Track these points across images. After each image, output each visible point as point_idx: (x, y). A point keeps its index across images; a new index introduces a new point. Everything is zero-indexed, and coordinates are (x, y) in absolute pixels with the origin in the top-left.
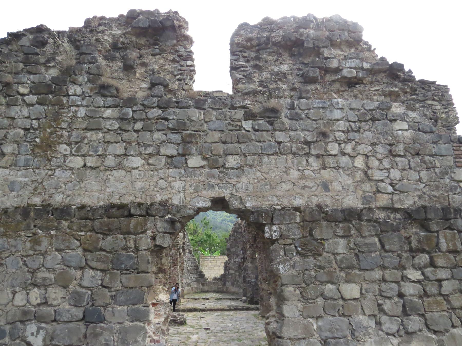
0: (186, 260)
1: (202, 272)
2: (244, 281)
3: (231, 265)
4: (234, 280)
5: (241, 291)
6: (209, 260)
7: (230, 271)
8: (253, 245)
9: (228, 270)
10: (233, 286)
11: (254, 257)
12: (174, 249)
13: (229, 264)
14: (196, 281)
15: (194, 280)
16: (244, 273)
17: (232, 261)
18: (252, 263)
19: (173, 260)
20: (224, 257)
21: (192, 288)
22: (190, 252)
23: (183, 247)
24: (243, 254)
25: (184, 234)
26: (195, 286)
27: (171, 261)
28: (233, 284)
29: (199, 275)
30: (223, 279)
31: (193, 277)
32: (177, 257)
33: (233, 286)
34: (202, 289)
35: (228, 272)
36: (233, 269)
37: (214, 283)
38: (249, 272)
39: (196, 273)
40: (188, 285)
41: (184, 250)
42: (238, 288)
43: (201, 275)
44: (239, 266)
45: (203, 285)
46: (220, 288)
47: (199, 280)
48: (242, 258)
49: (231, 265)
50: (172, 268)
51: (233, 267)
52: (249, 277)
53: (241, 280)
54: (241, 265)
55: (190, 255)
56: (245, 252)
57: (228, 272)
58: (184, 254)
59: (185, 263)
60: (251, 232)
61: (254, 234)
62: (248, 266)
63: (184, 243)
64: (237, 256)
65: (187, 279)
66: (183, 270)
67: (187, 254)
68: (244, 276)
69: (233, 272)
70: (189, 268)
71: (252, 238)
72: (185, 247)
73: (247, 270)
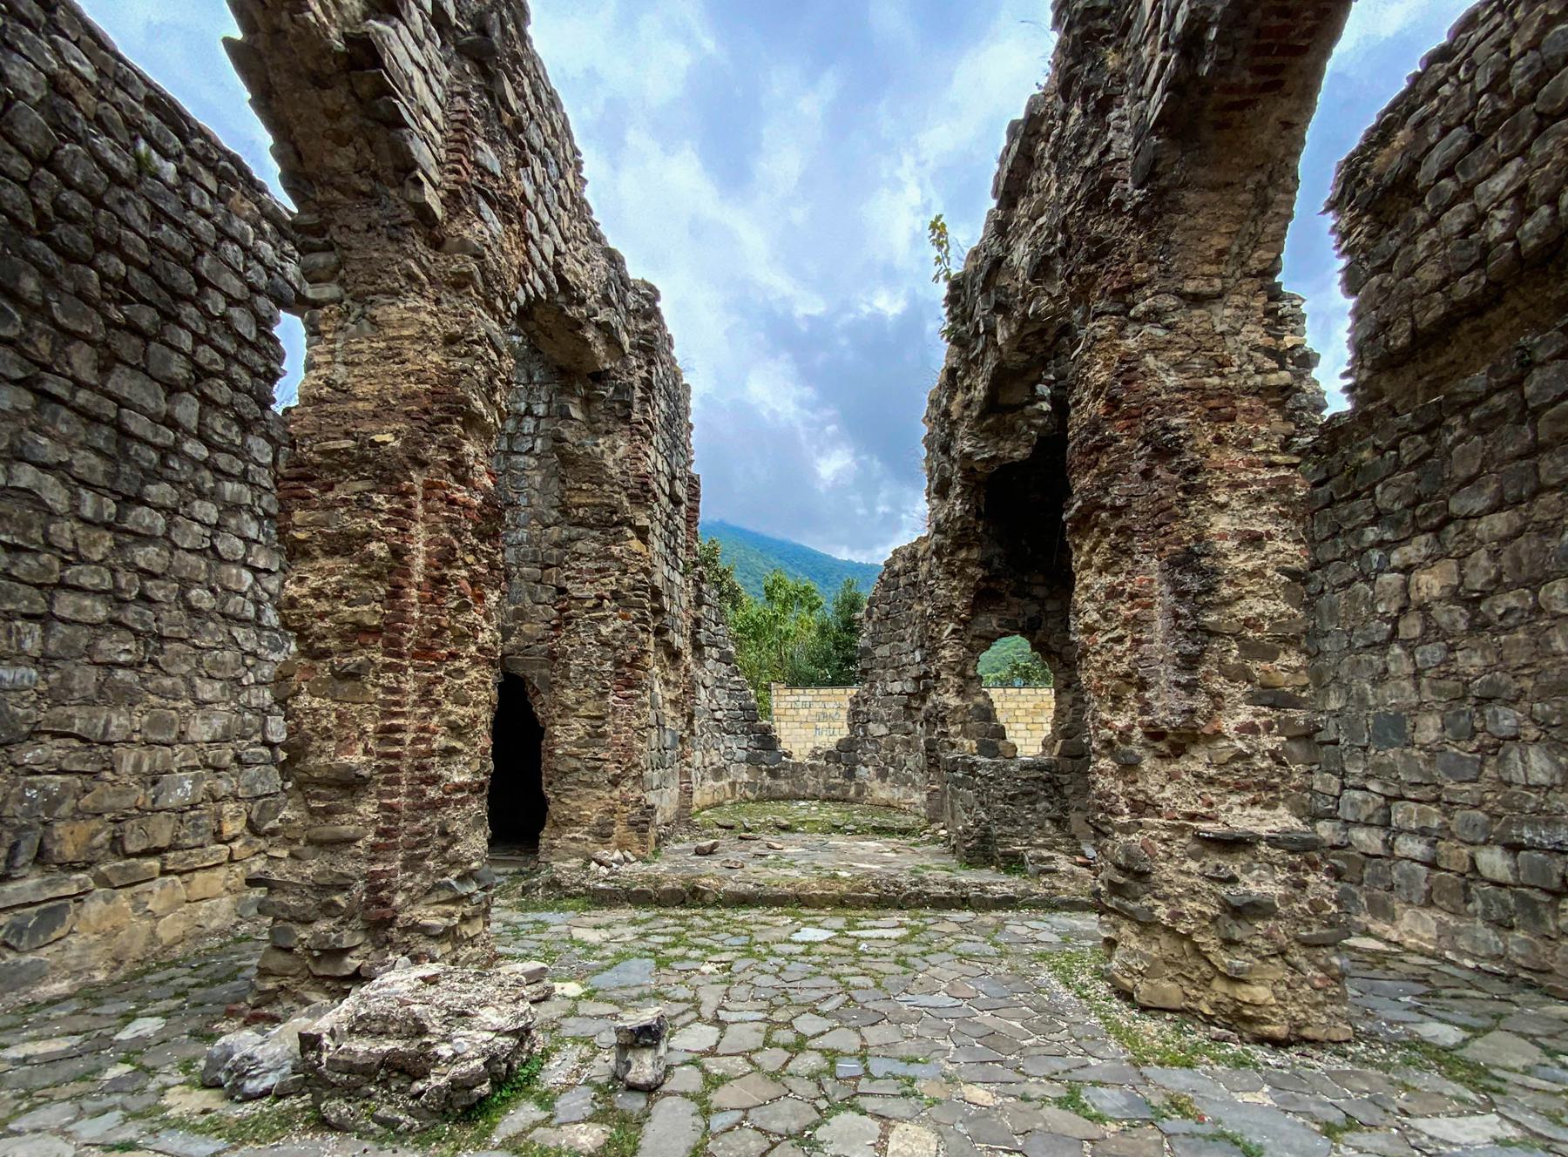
0: (708, 682)
1: (766, 731)
2: (933, 762)
3: (874, 707)
4: (884, 759)
5: (918, 798)
6: (802, 698)
7: (871, 725)
8: (963, 621)
9: (864, 725)
10: (883, 781)
11: (971, 673)
12: (624, 617)
13: (865, 701)
14: (747, 761)
15: (742, 754)
16: (928, 733)
17: (878, 691)
18: (961, 692)
19: (618, 663)
20: (849, 691)
21: (733, 784)
22: (725, 658)
23: (694, 634)
24: (924, 660)
25: (700, 590)
26: (745, 777)
27: (608, 666)
28: (882, 774)
29: (758, 740)
30: (845, 755)
31: (739, 746)
32: (635, 648)
33: (883, 781)
34: (769, 788)
35: (865, 731)
36: (882, 721)
37: (812, 767)
38: (953, 729)
39: (747, 734)
40: (718, 773)
41: (697, 647)
42: (903, 789)
43: (767, 741)
44: (907, 707)
45: (774, 774)
46: (834, 787)
47: (760, 756)
48: (917, 679)
49: (874, 707)
50: (610, 699)
51: (883, 712)
52: (953, 746)
53: (915, 760)
54: (915, 704)
55: (724, 669)
56: (931, 654)
57: (865, 731)
58: (700, 660)
59: (702, 693)
60: (961, 569)
61: (972, 578)
62: (946, 707)
63: (697, 622)
64: (900, 670)
65: (713, 752)
66: (691, 717)
67: (709, 664)
68: (929, 743)
69: (883, 730)
70: (719, 715)
71: (962, 595)
72: (703, 636)
73: (943, 720)
